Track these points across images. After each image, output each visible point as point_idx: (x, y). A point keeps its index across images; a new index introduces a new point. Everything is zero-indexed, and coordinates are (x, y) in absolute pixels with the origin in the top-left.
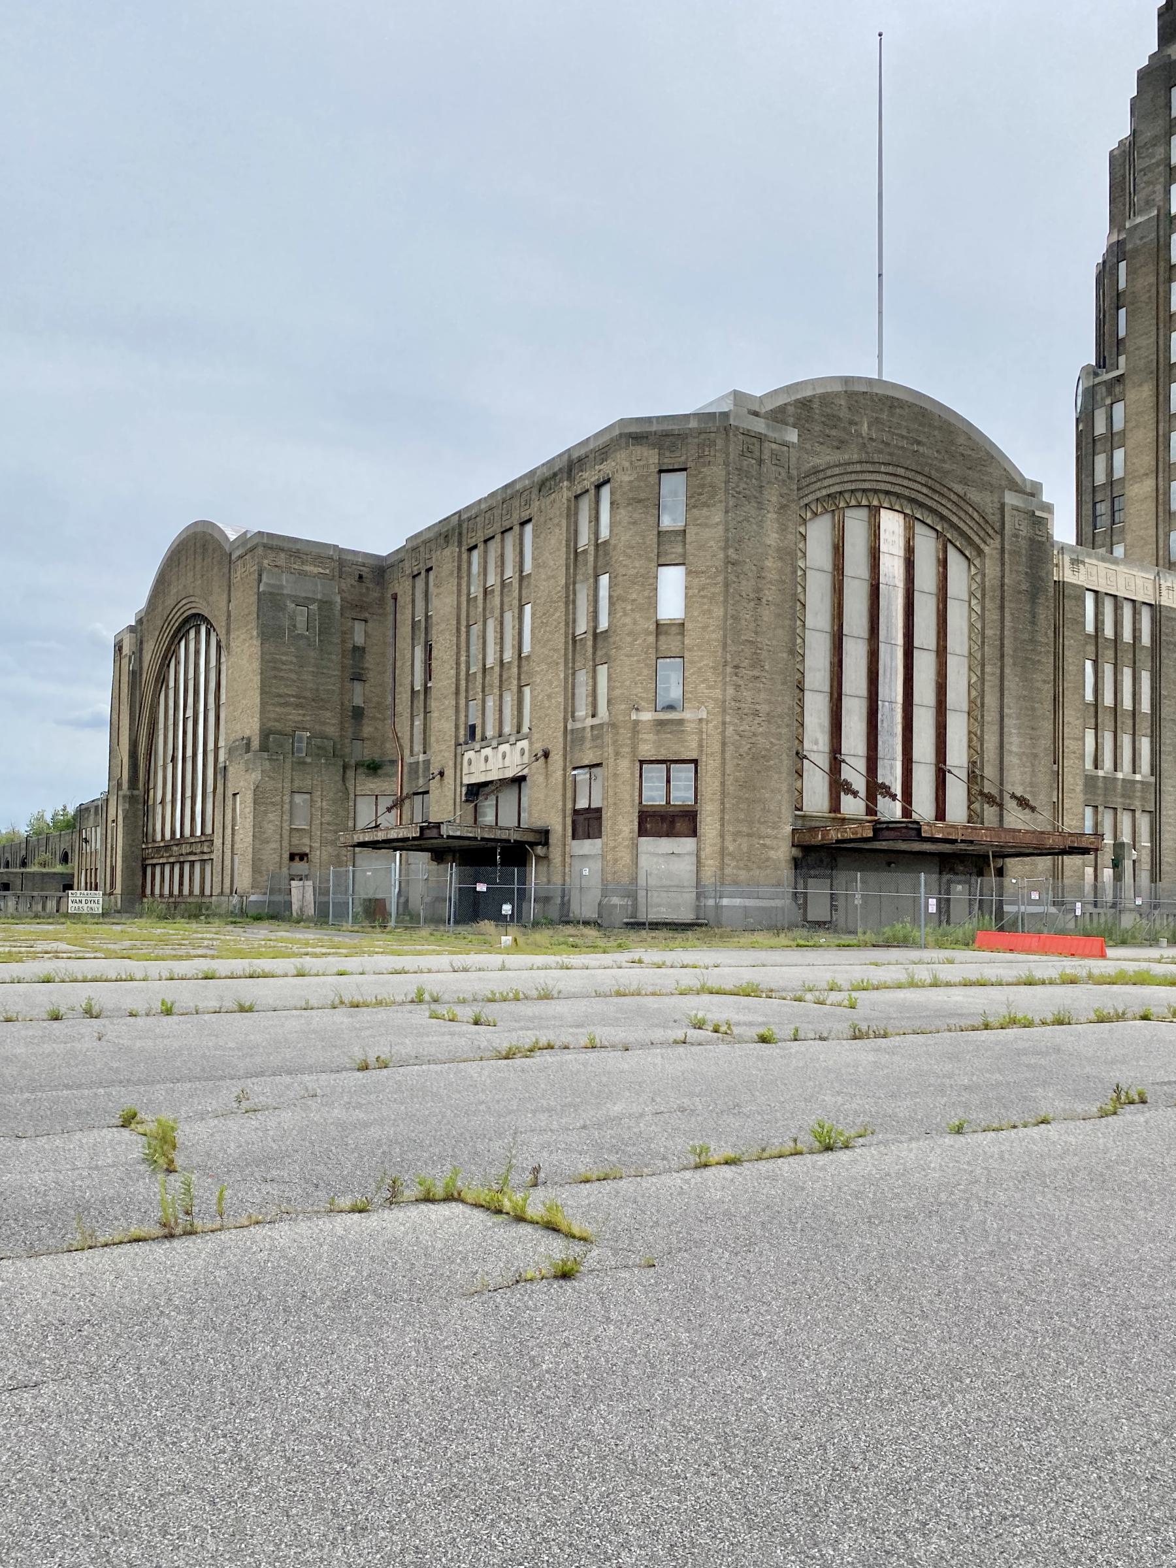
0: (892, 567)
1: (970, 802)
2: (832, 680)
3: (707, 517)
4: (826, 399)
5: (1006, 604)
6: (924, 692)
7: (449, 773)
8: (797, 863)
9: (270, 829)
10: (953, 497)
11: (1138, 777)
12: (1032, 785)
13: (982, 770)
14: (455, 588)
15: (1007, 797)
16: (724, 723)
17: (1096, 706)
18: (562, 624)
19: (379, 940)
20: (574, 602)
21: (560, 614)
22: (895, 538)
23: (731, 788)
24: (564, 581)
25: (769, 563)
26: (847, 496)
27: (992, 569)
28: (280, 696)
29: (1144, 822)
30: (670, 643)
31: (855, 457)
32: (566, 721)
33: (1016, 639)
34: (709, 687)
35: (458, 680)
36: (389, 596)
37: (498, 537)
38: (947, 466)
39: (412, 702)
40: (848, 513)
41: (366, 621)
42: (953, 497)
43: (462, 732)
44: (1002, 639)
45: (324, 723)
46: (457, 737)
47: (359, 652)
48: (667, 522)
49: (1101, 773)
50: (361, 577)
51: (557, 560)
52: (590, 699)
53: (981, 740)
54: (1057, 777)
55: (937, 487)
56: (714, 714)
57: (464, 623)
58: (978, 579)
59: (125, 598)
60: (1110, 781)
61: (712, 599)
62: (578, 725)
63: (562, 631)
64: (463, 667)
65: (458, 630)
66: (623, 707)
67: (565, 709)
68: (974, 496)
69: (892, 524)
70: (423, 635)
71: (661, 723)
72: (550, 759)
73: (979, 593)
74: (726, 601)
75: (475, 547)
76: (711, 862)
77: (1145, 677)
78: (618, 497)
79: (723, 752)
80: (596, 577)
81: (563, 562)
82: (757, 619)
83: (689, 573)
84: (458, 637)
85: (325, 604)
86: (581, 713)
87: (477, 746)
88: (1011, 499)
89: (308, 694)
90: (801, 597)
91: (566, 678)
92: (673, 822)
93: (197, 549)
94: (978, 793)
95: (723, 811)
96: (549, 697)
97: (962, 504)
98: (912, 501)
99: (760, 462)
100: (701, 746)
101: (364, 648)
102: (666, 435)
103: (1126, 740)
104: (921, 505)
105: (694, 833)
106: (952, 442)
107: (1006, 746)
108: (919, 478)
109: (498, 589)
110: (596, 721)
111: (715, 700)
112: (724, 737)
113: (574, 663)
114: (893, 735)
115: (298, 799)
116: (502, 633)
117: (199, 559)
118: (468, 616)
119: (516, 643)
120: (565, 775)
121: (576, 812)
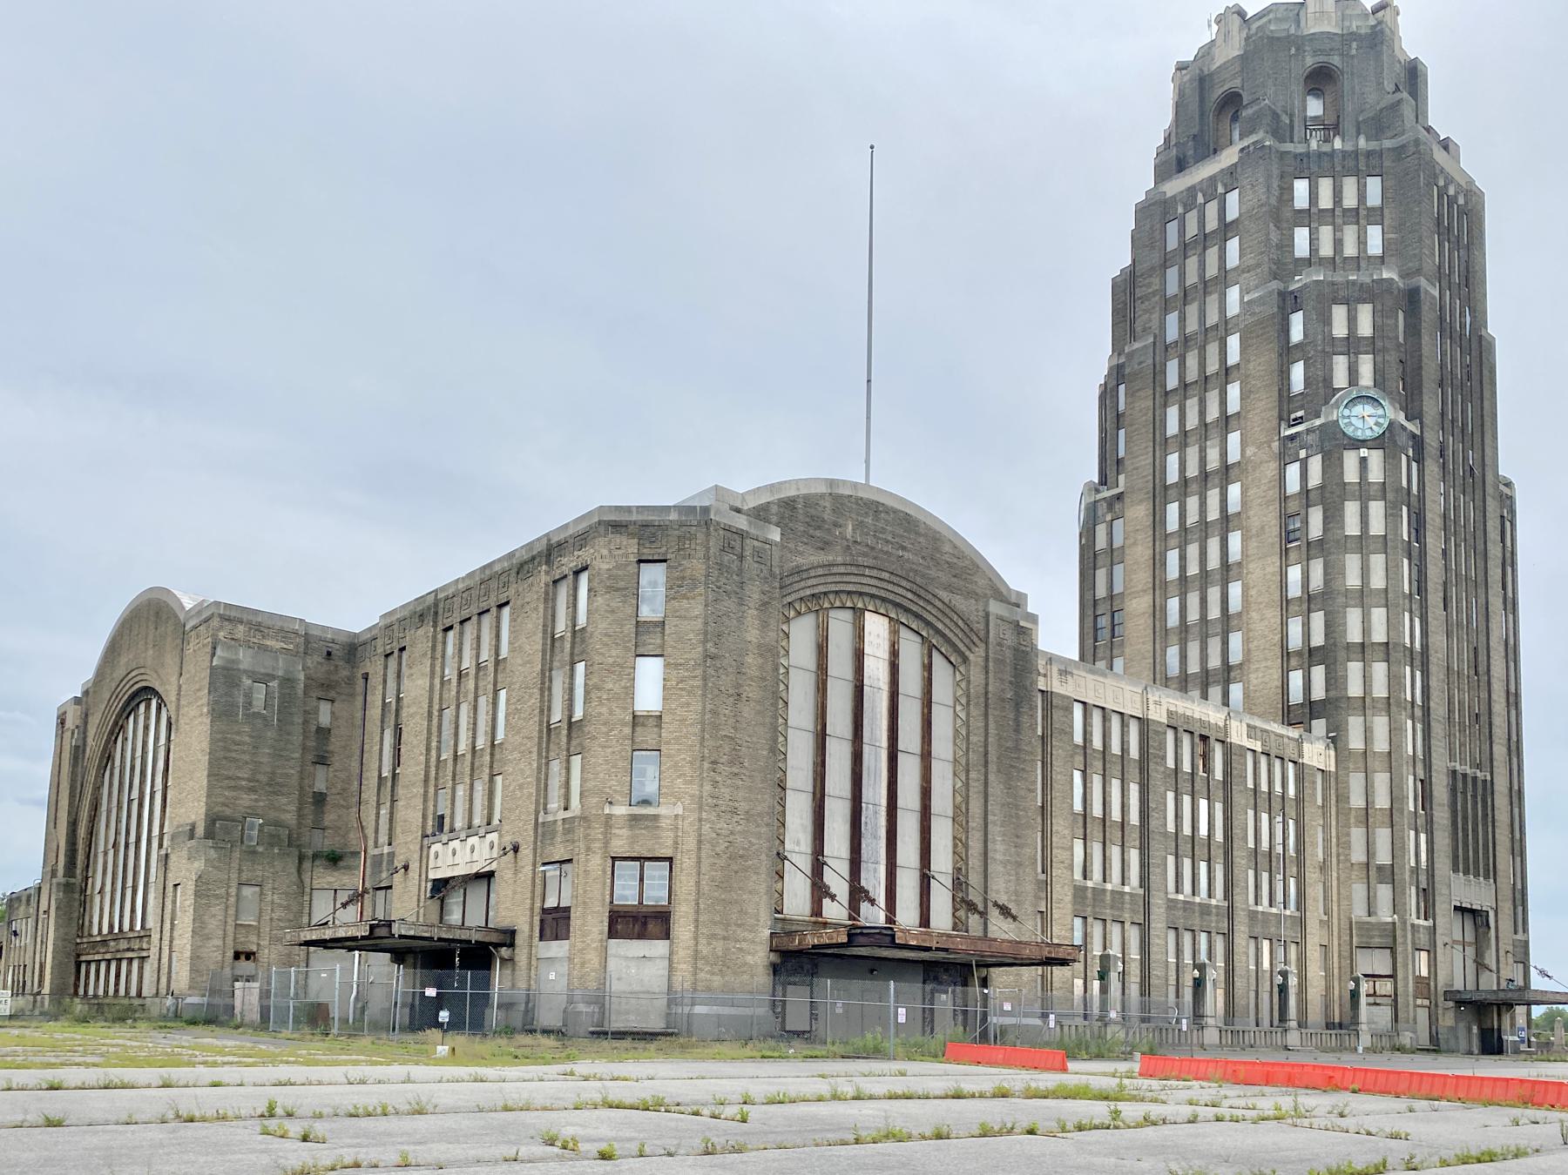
0: (877, 670)
1: (955, 910)
2: (815, 780)
3: (687, 610)
4: (810, 501)
6: (909, 796)
7: (414, 866)
9: (213, 924)
11: (1127, 889)
12: (1016, 893)
13: (967, 876)
15: (990, 904)
17: (1085, 816)
19: (317, 1047)
20: (550, 689)
21: (534, 701)
22: (880, 641)
25: (749, 660)
26: (831, 597)
27: (976, 676)
28: (229, 778)
29: (1134, 934)
31: (840, 559)
32: (537, 813)
33: (1000, 746)
35: (427, 766)
36: (359, 675)
38: (933, 573)
40: (832, 613)
41: (333, 701)
43: (430, 823)
44: (986, 746)
46: (424, 827)
47: (323, 733)
48: (646, 613)
49: (1090, 884)
50: (329, 654)
51: (534, 645)
53: (966, 846)
54: (1045, 886)
55: (922, 593)
58: (963, 685)
59: (71, 664)
60: (1099, 893)
64: (434, 753)
68: (959, 602)
69: (876, 628)
73: (965, 699)
74: (704, 695)
75: (451, 628)
76: (684, 966)
77: (1134, 789)
80: (573, 664)
81: (540, 647)
83: (667, 665)
85: (287, 681)
86: (553, 806)
87: (445, 838)
88: (995, 608)
90: (784, 695)
91: (539, 768)
92: (645, 924)
93: (151, 617)
94: (962, 903)
96: (521, 787)
97: (947, 611)
98: (897, 605)
99: (741, 557)
103: (1115, 852)
104: (907, 610)
105: (666, 935)
106: (937, 550)
107: (990, 854)
108: (904, 583)
109: (473, 672)
114: (875, 837)
115: (248, 892)
116: (475, 719)
117: (152, 627)
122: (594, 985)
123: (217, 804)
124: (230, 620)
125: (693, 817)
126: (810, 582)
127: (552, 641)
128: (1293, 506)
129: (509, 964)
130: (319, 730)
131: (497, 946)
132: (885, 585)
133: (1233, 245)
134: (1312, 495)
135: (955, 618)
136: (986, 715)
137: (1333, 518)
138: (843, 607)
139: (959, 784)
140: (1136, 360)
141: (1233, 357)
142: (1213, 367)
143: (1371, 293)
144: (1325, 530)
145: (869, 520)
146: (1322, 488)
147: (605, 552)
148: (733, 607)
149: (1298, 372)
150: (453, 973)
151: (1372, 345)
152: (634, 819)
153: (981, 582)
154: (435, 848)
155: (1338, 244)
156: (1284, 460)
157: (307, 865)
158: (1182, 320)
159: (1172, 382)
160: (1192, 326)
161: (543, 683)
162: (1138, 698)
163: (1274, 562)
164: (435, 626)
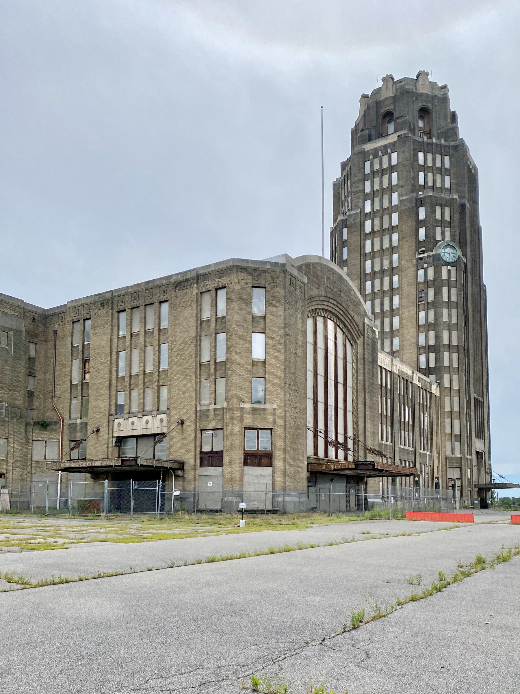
4: (314, 265)
5: (366, 366)
8: (309, 480)
10: (350, 317)
14: (109, 331)
16: (285, 411)
18: (194, 356)
20: (200, 345)
21: (192, 349)
23: (288, 442)
27: (360, 350)
37: (142, 308)
39: (71, 390)
40: (318, 317)
42: (350, 317)
43: (113, 408)
44: (364, 381)
53: (358, 426)
55: (346, 312)
56: (280, 407)
62: (204, 408)
63: (194, 359)
65: (111, 353)
66: (236, 400)
67: (196, 400)
69: (330, 324)
71: (254, 410)
72: (184, 425)
78: (232, 295)
84: (111, 357)
95: (285, 453)
97: (352, 321)
100: (274, 421)
101: (35, 359)
106: (350, 293)
110: (217, 407)
113: (200, 376)
118: (118, 346)
121: (201, 453)
127: (201, 323)
128: (421, 287)
129: (181, 479)
131: (174, 470)
132: (334, 307)
134: (429, 283)
135: (355, 324)
137: (438, 293)
138: (321, 316)
139: (354, 398)
146: (434, 280)
150: (136, 484)
153: (362, 309)
154: (117, 421)
157: (30, 428)
161: (197, 342)
163: (413, 309)
164: (112, 309)
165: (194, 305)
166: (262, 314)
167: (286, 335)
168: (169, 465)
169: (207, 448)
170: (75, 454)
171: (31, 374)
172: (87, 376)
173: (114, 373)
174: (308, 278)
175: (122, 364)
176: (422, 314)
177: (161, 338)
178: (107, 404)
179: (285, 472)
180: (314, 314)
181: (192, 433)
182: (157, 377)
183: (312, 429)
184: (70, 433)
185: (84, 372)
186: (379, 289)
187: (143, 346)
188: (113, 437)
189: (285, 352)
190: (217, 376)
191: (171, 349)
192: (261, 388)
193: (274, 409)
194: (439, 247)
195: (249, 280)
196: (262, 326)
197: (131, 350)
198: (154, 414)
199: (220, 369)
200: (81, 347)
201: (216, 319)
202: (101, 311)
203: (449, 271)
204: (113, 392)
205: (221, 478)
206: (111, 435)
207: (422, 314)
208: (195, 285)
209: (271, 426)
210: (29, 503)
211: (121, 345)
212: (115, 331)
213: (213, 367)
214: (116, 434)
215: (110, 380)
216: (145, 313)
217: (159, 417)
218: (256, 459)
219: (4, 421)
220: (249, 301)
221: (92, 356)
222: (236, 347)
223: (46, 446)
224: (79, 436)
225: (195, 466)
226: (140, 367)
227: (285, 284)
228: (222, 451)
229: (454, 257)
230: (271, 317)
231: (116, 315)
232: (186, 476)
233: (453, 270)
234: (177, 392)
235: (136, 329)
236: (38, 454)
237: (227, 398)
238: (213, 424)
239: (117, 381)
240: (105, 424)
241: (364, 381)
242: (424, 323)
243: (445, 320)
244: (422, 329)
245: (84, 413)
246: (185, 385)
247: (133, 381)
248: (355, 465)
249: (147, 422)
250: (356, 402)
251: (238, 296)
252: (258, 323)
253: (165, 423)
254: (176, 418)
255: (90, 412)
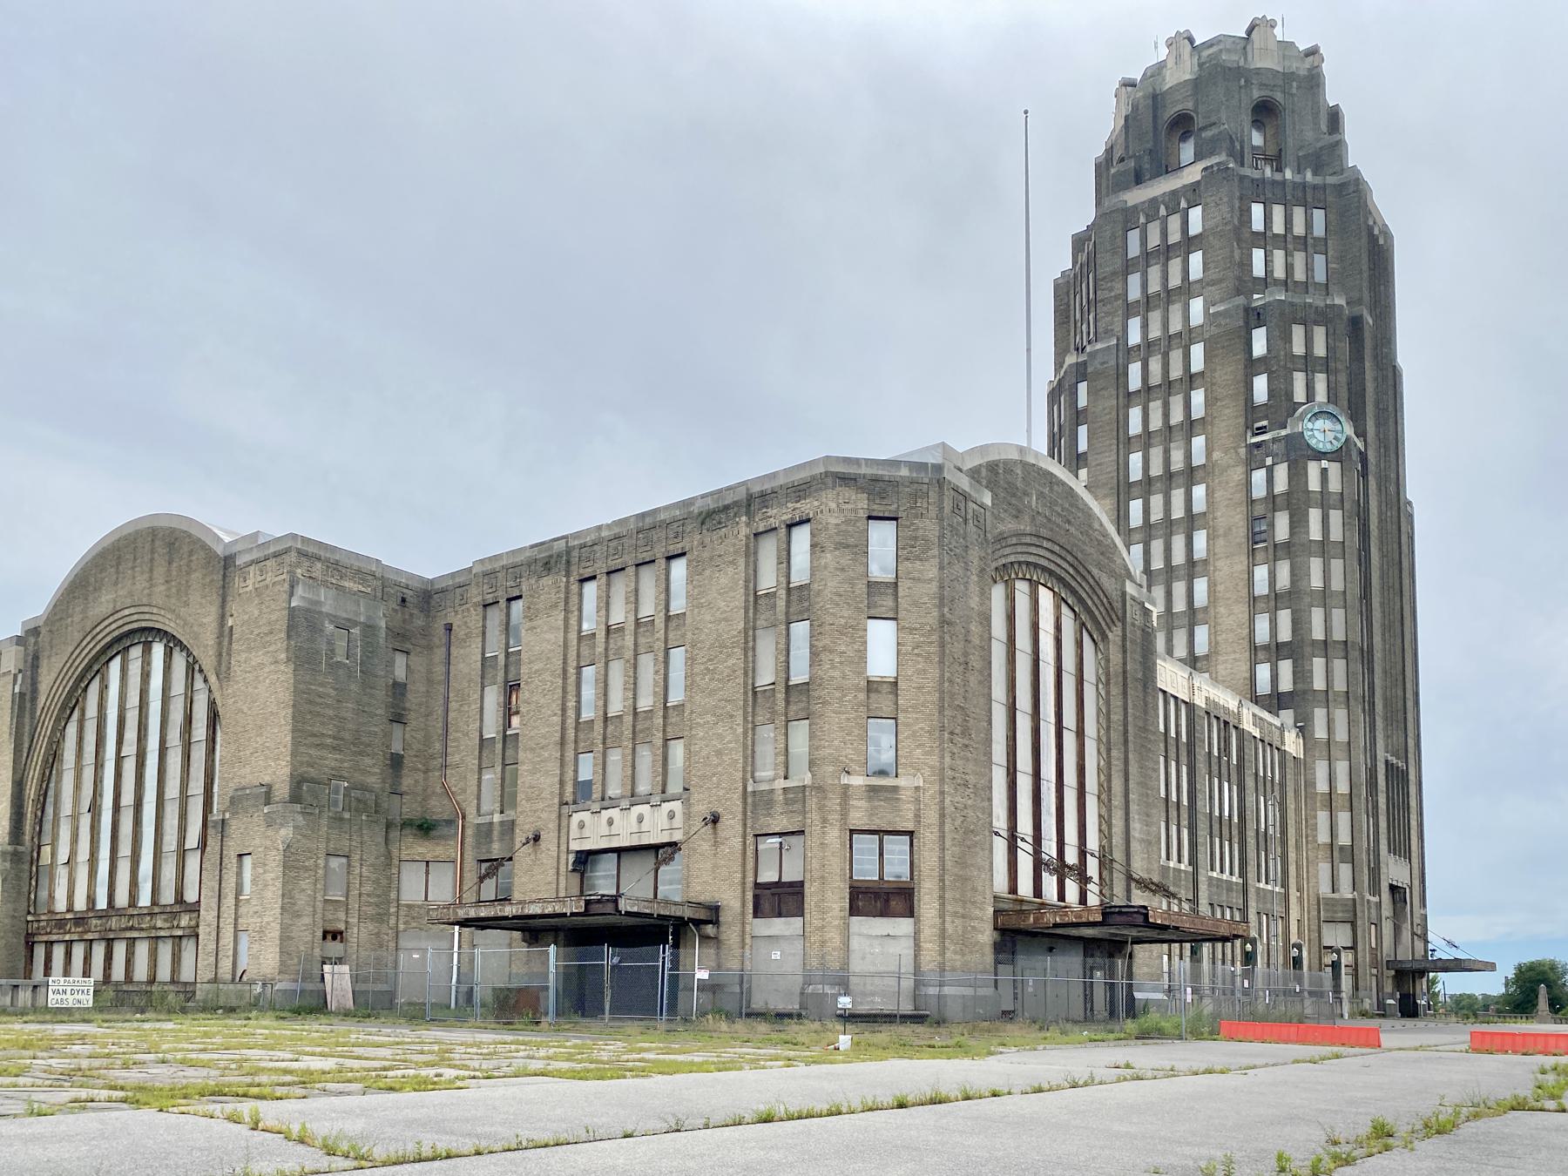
3: (920, 572)
4: (1008, 466)
5: (1130, 691)
9: (302, 900)
14: (561, 623)
18: (740, 672)
20: (754, 649)
21: (736, 660)
23: (949, 865)
24: (742, 625)
27: (1116, 657)
30: (884, 703)
34: (926, 753)
37: (631, 570)
43: (569, 789)
44: (1125, 725)
45: (364, 772)
52: (781, 758)
55: (1081, 569)
57: (572, 664)
61: (927, 659)
66: (831, 769)
67: (744, 771)
69: (1046, 598)
70: (501, 674)
78: (822, 538)
79: (942, 824)
82: (966, 682)
84: (565, 678)
89: (347, 736)
91: (745, 733)
95: (943, 889)
99: (966, 520)
100: (917, 817)
102: (875, 480)
106: (1090, 526)
111: (932, 767)
112: (943, 809)
114: (1049, 813)
115: (335, 863)
119: (660, 690)
120: (744, 843)
121: (757, 885)
122: (837, 965)
123: (302, 763)
124: (307, 558)
125: (933, 790)
126: (1008, 550)
127: (755, 600)
128: (1259, 510)
129: (712, 943)
130: (396, 684)
131: (698, 923)
133: (1196, 259)
134: (1278, 500)
136: (1125, 693)
140: (1100, 358)
141: (1197, 364)
142: (1176, 372)
143: (1324, 317)
144: (1292, 534)
145: (1046, 491)
146: (1288, 494)
147: (833, 505)
148: (961, 572)
149: (1261, 385)
150: (616, 957)
151: (1326, 365)
152: (873, 790)
153: (1119, 561)
154: (576, 818)
155: (1289, 268)
156: (1251, 464)
157: (395, 834)
158: (1145, 326)
159: (1135, 383)
160: (1155, 332)
161: (746, 642)
162: (1185, 683)
163: (1241, 562)
164: (568, 575)
165: (742, 562)
166: (890, 577)
167: (943, 622)
168: (687, 913)
169: (768, 875)
170: (489, 890)
171: (398, 719)
172: (515, 720)
173: (571, 713)
174: (995, 496)
175: (588, 693)
176: (1261, 573)
177: (671, 635)
178: (557, 779)
179: (943, 930)
180: (1004, 574)
181: (737, 842)
182: (661, 721)
183: (1004, 834)
184: (478, 845)
185: (508, 712)
186: (1161, 516)
187: (631, 653)
188: (568, 852)
189: (941, 662)
190: (791, 714)
191: (691, 660)
192: (887, 740)
193: (917, 788)
194: (1301, 418)
195: (861, 503)
196: (890, 603)
197: (607, 664)
198: (656, 800)
199: (797, 699)
200: (502, 658)
201: (789, 590)
202: (547, 581)
203: (1324, 472)
204: (570, 754)
205: (799, 945)
206: (564, 848)
207: (1261, 573)
208: (744, 518)
209: (910, 826)
210: (392, 995)
211: (585, 651)
212: (573, 621)
213: (781, 696)
214: (575, 846)
215: (563, 729)
216: (637, 582)
217: (667, 806)
218: (880, 899)
219: (342, 819)
220: (860, 550)
221: (524, 677)
222: (831, 652)
223: (427, 873)
224: (496, 850)
225: (743, 914)
226: (625, 700)
227: (941, 509)
228: (802, 883)
229: (1336, 438)
230: (909, 583)
231: (574, 587)
232: (723, 937)
233: (1334, 469)
234: (704, 753)
235: (618, 615)
236: (412, 887)
237: (812, 764)
238: (781, 823)
239: (576, 729)
240: (553, 826)
241: (1125, 725)
242: (1266, 592)
243: (1316, 582)
244: (1260, 605)
245: (507, 799)
246: (720, 737)
247: (610, 728)
248: (1103, 914)
249: (640, 819)
250: (1105, 772)
251: (838, 539)
252: (880, 598)
253: (678, 821)
254: (702, 809)
255: (520, 796)
